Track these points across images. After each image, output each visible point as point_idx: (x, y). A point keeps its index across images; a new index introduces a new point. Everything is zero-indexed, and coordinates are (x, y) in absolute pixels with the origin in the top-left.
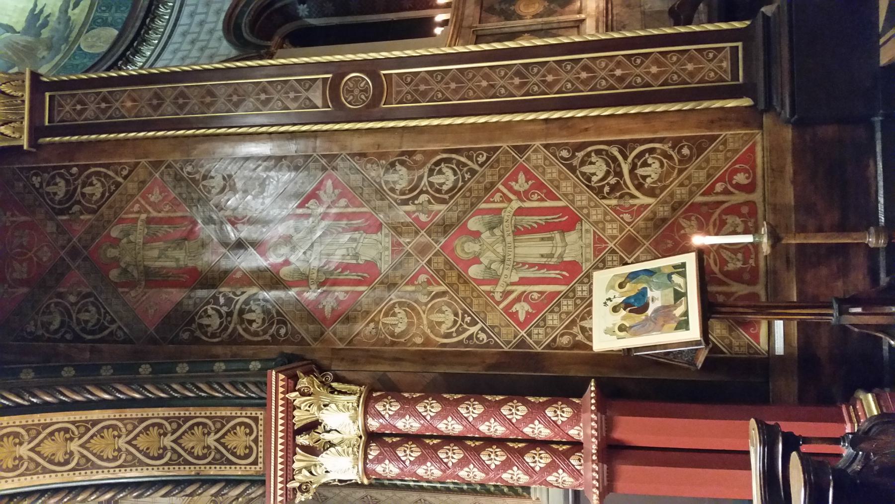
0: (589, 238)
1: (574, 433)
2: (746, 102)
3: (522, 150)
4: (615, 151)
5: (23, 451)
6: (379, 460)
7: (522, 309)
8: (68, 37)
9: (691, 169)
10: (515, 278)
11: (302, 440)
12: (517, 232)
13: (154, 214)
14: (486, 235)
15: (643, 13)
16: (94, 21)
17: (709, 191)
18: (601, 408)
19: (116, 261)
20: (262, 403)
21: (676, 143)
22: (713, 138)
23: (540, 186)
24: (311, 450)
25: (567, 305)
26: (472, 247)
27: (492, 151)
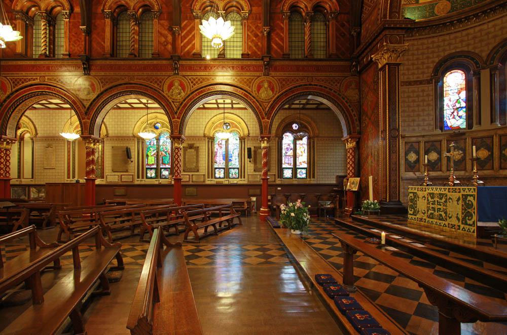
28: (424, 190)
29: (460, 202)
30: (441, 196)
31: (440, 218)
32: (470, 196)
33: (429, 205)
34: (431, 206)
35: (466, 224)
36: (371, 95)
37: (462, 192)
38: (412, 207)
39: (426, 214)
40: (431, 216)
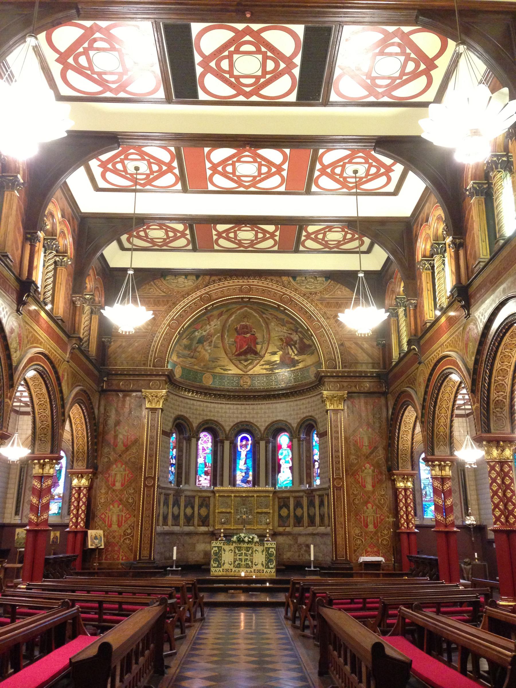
0: (116, 529)
2: (138, 559)
3: (134, 516)
5: (79, 428)
6: (76, 490)
7: (103, 516)
8: (208, 369)
10: (110, 515)
12: (118, 516)
13: (129, 437)
14: (118, 509)
15: (195, 544)
16: (215, 375)
17: (122, 552)
20: (87, 468)
21: (132, 546)
22: (132, 553)
23: (127, 520)
25: (103, 525)
26: (116, 505)
27: (135, 510)
29: (264, 553)
31: (247, 566)
33: (235, 557)
34: (238, 557)
35: (269, 568)
38: (216, 560)
39: (232, 565)
40: (239, 566)
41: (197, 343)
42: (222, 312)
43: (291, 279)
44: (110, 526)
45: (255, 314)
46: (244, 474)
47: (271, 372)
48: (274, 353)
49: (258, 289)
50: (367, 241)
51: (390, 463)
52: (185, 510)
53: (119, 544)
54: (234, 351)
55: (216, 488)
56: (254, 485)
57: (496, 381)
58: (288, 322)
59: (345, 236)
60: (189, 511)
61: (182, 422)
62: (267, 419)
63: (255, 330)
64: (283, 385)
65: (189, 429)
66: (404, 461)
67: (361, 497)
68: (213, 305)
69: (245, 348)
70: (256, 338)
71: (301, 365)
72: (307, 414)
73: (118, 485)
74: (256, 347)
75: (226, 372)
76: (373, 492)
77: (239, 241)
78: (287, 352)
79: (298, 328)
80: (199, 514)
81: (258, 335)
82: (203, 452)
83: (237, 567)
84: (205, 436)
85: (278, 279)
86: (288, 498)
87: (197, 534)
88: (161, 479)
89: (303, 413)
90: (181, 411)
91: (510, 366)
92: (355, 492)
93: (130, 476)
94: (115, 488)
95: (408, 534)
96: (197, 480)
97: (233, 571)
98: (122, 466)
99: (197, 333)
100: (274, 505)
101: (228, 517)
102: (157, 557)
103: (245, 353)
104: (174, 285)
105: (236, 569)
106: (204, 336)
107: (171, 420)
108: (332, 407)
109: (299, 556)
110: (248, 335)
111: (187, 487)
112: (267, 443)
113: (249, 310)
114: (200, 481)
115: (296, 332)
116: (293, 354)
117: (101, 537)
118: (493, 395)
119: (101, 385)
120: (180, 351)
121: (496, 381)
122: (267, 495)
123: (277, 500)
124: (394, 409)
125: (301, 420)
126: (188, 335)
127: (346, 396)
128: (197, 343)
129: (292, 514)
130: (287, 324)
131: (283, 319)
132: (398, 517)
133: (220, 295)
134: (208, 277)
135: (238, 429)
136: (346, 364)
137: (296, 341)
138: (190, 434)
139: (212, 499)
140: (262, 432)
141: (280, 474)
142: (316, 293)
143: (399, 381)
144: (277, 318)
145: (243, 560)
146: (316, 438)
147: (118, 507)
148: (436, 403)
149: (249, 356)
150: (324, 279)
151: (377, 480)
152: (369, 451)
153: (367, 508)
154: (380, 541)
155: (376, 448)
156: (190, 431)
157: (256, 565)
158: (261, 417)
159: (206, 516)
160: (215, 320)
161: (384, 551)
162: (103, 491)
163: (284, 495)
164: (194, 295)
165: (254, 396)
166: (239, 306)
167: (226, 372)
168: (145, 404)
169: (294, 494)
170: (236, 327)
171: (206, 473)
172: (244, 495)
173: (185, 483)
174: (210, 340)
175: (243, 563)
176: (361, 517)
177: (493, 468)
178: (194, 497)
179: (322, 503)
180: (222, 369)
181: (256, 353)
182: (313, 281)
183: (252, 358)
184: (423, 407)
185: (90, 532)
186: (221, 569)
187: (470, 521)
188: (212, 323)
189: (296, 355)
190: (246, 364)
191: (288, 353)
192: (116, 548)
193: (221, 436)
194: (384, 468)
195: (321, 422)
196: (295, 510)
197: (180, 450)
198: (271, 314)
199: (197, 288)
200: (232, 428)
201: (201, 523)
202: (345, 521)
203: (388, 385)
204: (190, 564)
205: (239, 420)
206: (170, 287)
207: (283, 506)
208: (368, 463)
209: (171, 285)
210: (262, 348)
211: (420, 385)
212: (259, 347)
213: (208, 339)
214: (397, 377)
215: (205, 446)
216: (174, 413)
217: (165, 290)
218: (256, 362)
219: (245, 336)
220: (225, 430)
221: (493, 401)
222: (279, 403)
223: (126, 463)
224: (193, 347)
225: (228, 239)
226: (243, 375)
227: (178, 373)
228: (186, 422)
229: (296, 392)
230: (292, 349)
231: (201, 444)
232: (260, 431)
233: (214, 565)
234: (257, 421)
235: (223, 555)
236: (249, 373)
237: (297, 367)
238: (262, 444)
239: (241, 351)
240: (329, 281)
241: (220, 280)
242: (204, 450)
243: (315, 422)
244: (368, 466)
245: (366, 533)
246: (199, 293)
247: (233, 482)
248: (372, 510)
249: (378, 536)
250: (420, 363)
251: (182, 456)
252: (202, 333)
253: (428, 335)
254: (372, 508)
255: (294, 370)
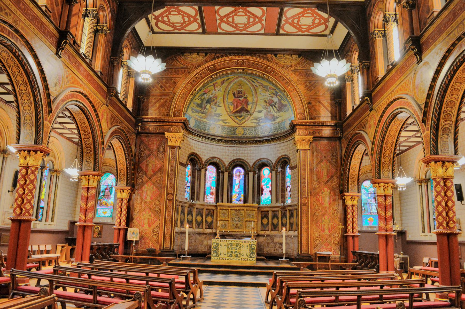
0: (147, 228)
1: (121, 225)
2: (162, 248)
4: (158, 232)
5: (121, 158)
6: (119, 200)
7: (138, 219)
9: (155, 242)
11: (122, 190)
12: (149, 219)
18: (124, 229)
19: (150, 159)
20: (127, 186)
21: (158, 240)
23: (155, 222)
24: (120, 192)
25: (138, 225)
26: (147, 212)
28: (225, 241)
30: (237, 245)
31: (237, 256)
32: (254, 244)
33: (229, 250)
35: (251, 257)
36: (154, 159)
37: (249, 243)
38: (215, 252)
40: (231, 256)
41: (206, 103)
42: (224, 81)
43: (273, 55)
44: (143, 226)
45: (248, 83)
46: (237, 195)
47: (257, 125)
48: (260, 112)
49: (249, 63)
50: (332, 20)
51: (342, 187)
52: (196, 217)
53: (150, 238)
54: (232, 109)
55: (218, 204)
56: (244, 202)
57: (445, 112)
58: (271, 89)
59: (314, 21)
60: (199, 218)
61: (194, 157)
62: (254, 158)
63: (247, 95)
64: (266, 134)
65: (200, 163)
66: (353, 186)
67: (321, 211)
68: (216, 74)
69: (240, 108)
70: (247, 101)
71: (279, 120)
72: (283, 154)
73: (148, 199)
74: (247, 107)
75: (226, 125)
76: (329, 208)
77: (236, 24)
78: (269, 110)
79: (277, 93)
80: (206, 221)
81: (250, 99)
82: (209, 179)
83: (229, 257)
84: (211, 168)
85: (264, 56)
86: (269, 211)
87: (204, 234)
88: (178, 195)
89: (280, 153)
90: (194, 150)
91: (458, 98)
92: (316, 208)
93: (157, 192)
94: (146, 200)
95: (353, 237)
96: (205, 198)
97: (227, 259)
98: (151, 186)
99: (205, 96)
100: (258, 216)
101: (226, 223)
102: (176, 248)
103: (240, 111)
104: (189, 59)
105: (229, 258)
106: (211, 98)
107: (187, 155)
108: (301, 148)
109: (275, 250)
110: (242, 99)
111: (198, 202)
112: (254, 174)
113: (243, 80)
114: (207, 199)
115: (276, 95)
116: (274, 112)
117: (137, 233)
118: (442, 124)
119: (137, 129)
120: (194, 108)
121: (445, 112)
122: (253, 209)
123: (260, 213)
124: (347, 148)
125: (278, 158)
126: (200, 96)
127: (312, 139)
128: (206, 103)
129: (270, 222)
130: (269, 90)
131: (267, 86)
132: (346, 225)
133: (222, 66)
134: (213, 54)
135: (234, 164)
136: (312, 117)
137: (276, 102)
138: (201, 166)
139: (215, 211)
140: (251, 166)
141: (262, 195)
142: (291, 66)
143: (351, 128)
144: (262, 85)
145: (234, 252)
146: (288, 170)
147: (149, 213)
148: (383, 138)
149: (242, 114)
150: (297, 56)
151: (332, 199)
152: (327, 179)
153: (324, 219)
154: (332, 241)
155: (332, 177)
156: (200, 164)
157: (242, 255)
158: (250, 156)
159: (211, 222)
160: (219, 87)
161: (335, 248)
162: (138, 202)
163: (265, 209)
164: (204, 67)
165: (246, 141)
166: (236, 76)
167: (226, 125)
168: (167, 143)
169: (272, 209)
170: (233, 92)
171: (212, 194)
172: (237, 209)
173: (197, 199)
174: (215, 101)
175: (234, 254)
176: (320, 225)
177: (438, 183)
178: (203, 209)
179: (292, 215)
180: (223, 122)
181: (247, 111)
182: (289, 57)
183: (244, 115)
184: (373, 143)
185: (129, 229)
186: (218, 258)
187: (397, 227)
188: (216, 89)
189: (276, 112)
190: (240, 119)
191: (270, 111)
192: (148, 241)
193: (222, 169)
194: (338, 191)
195: (293, 159)
196: (272, 219)
197: (193, 177)
198: (258, 82)
199: (206, 62)
200: (231, 163)
201: (207, 227)
202: (308, 228)
203: (342, 132)
204: (199, 253)
205: (235, 158)
206: (187, 61)
207: (264, 217)
208: (326, 187)
209: (187, 59)
210: (251, 108)
211: (370, 127)
212: (249, 107)
213: (213, 101)
214: (349, 126)
215: (211, 175)
216: (189, 151)
217: (183, 63)
218: (247, 118)
219: (240, 99)
220: (225, 165)
221: (441, 128)
222: (263, 146)
223: (154, 184)
224: (203, 106)
225: (228, 23)
226: (239, 126)
227: (192, 124)
228: (198, 158)
229: (275, 138)
230: (273, 108)
231: (208, 174)
232: (250, 165)
233: (214, 255)
234: (248, 159)
235: (220, 248)
236: (241, 125)
237: (276, 121)
238: (251, 174)
239: (237, 109)
240: (301, 57)
241: (222, 56)
242: (210, 177)
243: (289, 159)
244: (326, 189)
245: (323, 235)
246: (207, 65)
247: (230, 200)
248: (328, 220)
249: (331, 238)
250: (371, 111)
251: (195, 181)
252: (209, 96)
253: (379, 87)
254: (328, 219)
255: (274, 123)
